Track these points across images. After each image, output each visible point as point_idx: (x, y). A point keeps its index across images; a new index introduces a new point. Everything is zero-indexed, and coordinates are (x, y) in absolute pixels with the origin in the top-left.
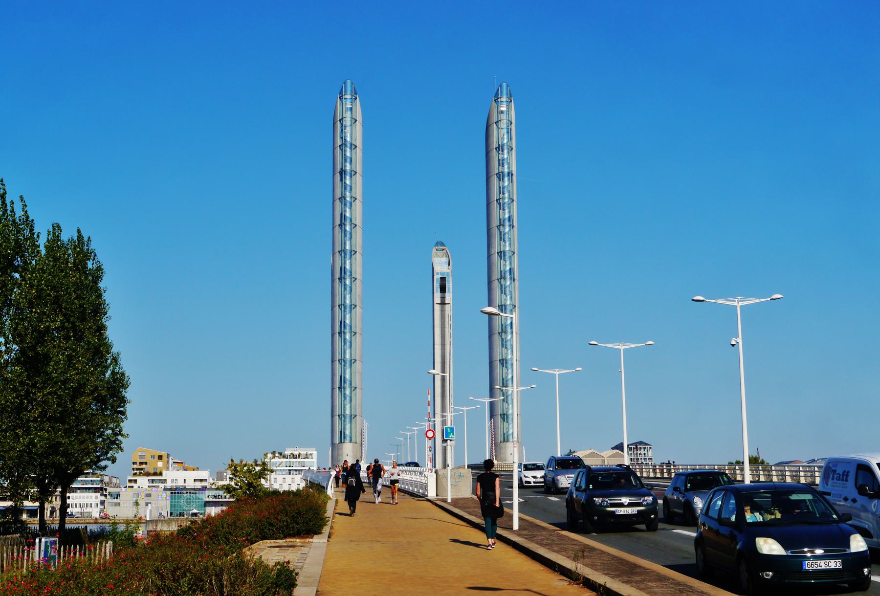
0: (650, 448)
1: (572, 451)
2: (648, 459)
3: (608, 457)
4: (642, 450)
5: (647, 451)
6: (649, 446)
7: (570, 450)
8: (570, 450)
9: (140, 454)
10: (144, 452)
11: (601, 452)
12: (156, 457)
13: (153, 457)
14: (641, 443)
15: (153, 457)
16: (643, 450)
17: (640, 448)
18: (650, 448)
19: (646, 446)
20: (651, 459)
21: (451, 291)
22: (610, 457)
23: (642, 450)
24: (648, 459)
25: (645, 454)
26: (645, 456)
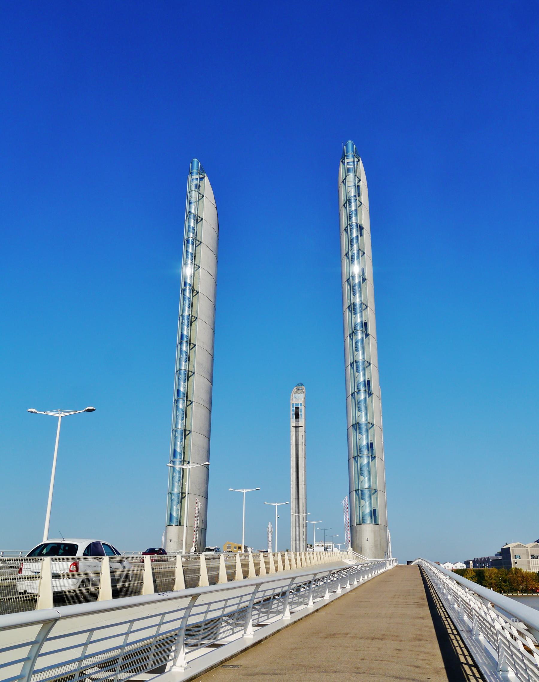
1: (507, 544)
3: (530, 548)
9: (228, 546)
10: (230, 545)
11: (525, 545)
12: (237, 548)
13: (235, 548)
15: (235, 548)
21: (303, 417)
22: (532, 547)
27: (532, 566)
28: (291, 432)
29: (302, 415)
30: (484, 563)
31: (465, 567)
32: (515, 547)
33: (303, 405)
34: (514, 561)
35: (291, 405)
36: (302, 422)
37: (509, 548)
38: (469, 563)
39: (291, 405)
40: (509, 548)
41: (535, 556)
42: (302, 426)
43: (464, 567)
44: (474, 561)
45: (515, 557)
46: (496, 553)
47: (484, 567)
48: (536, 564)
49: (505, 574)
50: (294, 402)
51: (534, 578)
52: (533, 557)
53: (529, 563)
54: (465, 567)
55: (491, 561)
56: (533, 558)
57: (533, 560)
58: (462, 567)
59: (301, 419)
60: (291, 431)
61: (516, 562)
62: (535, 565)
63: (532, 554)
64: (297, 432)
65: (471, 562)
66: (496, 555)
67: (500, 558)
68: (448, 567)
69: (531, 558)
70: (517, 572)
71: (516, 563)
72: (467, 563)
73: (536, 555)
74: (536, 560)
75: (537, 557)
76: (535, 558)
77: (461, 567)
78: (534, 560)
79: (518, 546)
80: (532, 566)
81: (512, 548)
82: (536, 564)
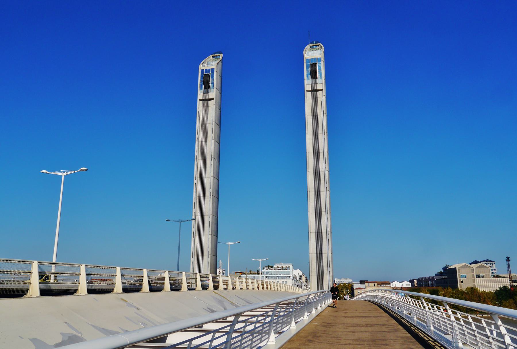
0: (494, 263)
1: (447, 265)
2: (493, 270)
4: (489, 264)
5: (493, 265)
6: (493, 262)
7: (446, 265)
8: (446, 265)
14: (487, 260)
16: (490, 264)
17: (488, 263)
18: (494, 263)
19: (492, 262)
20: (495, 269)
22: (477, 268)
23: (489, 264)
24: (493, 270)
25: (491, 267)
26: (491, 268)
27: (477, 285)
28: (198, 107)
29: (213, 83)
30: (428, 282)
31: (410, 286)
32: (461, 267)
33: (215, 70)
34: (460, 280)
35: (200, 71)
36: (213, 93)
37: (456, 268)
38: (414, 282)
39: (200, 71)
40: (456, 268)
41: (480, 276)
42: (213, 99)
43: (409, 285)
44: (418, 280)
45: (462, 277)
46: (436, 273)
47: (429, 285)
48: (481, 283)
49: (460, 294)
50: (204, 68)
51: (492, 298)
52: (478, 276)
53: (474, 282)
54: (410, 286)
55: (436, 280)
56: (478, 278)
57: (477, 279)
58: (408, 285)
59: (212, 89)
60: (198, 105)
61: (462, 281)
62: (480, 284)
63: (478, 274)
64: (206, 108)
65: (415, 281)
66: (436, 275)
67: (444, 277)
68: (396, 285)
69: (476, 278)
70: (473, 292)
71: (462, 282)
72: (412, 281)
73: (481, 275)
74: (481, 279)
75: (482, 276)
76: (480, 278)
77: (407, 285)
78: (479, 279)
79: (465, 267)
80: (477, 285)
81: (458, 268)
82: (481, 283)
